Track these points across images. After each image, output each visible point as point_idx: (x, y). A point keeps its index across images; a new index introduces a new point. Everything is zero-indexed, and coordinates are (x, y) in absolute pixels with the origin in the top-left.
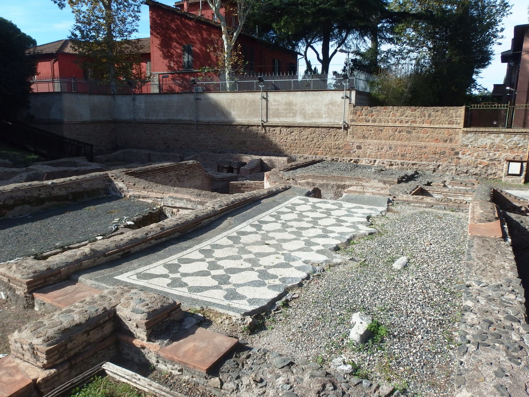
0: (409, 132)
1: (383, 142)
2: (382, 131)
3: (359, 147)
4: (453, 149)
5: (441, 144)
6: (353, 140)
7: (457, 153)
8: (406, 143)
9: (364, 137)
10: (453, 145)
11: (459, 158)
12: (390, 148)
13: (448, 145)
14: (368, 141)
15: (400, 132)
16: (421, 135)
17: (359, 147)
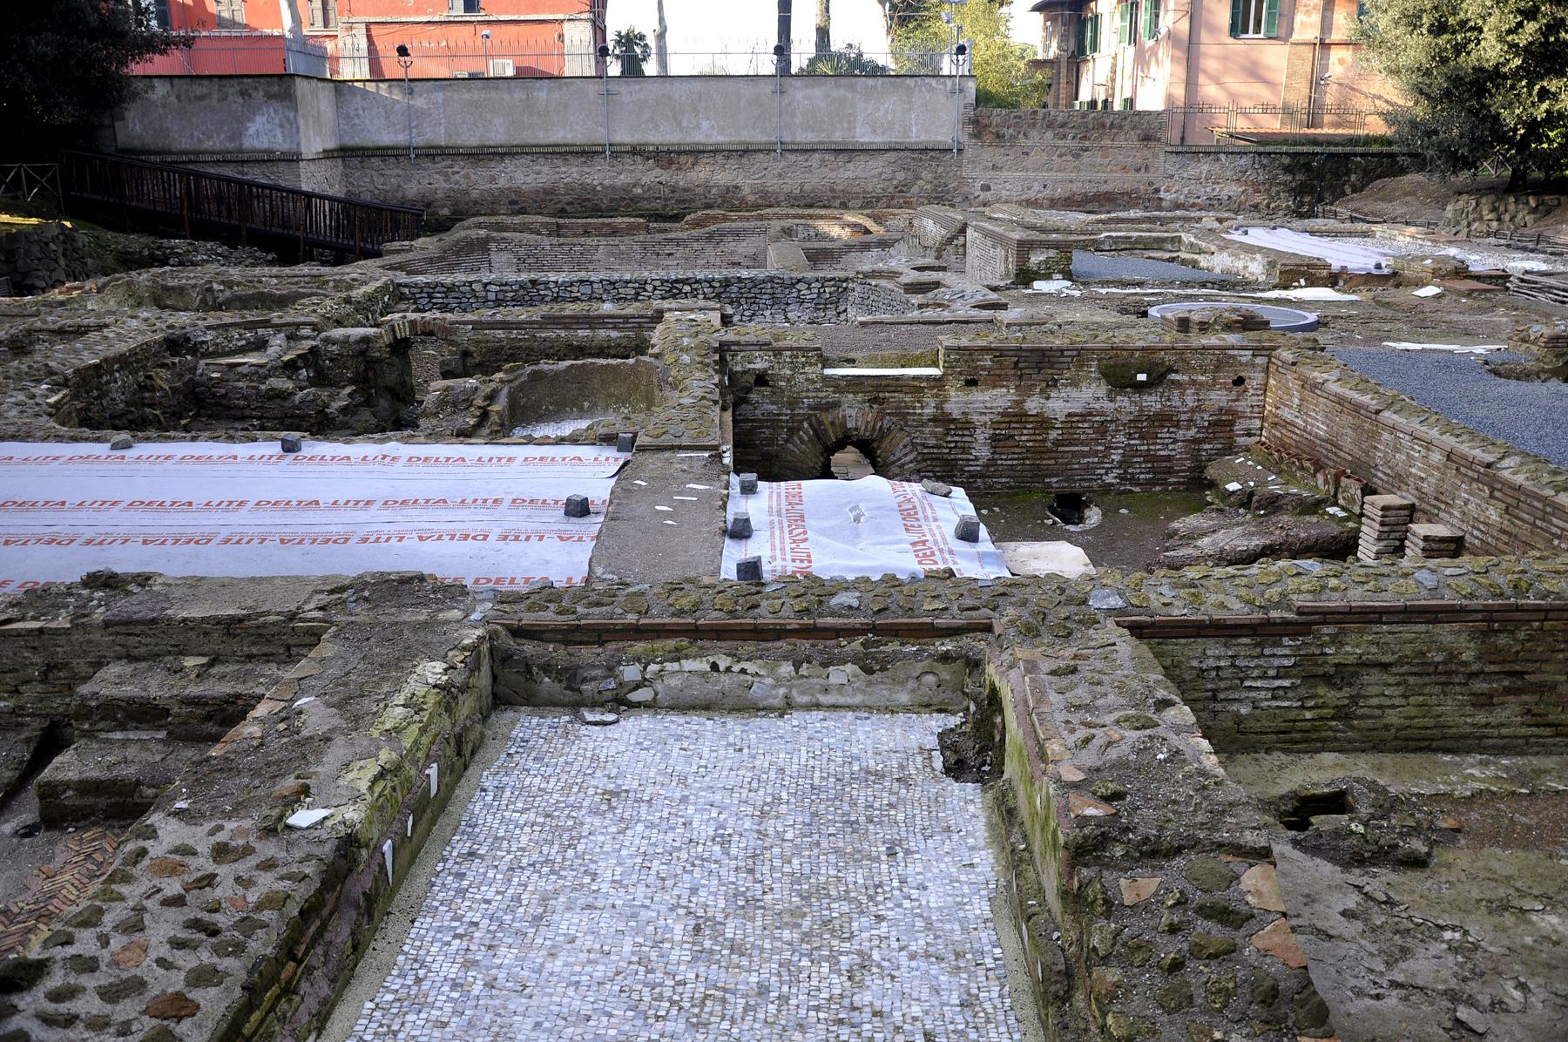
0: (1077, 156)
1: (1032, 175)
2: (1027, 154)
3: (986, 188)
4: (1151, 184)
5: (1132, 175)
6: (974, 175)
7: (1157, 191)
8: (1073, 176)
9: (994, 167)
10: (1151, 176)
11: (1161, 199)
12: (1045, 186)
13: (1142, 175)
14: (1004, 174)
15: (1060, 156)
16: (1099, 160)
17: (986, 188)
